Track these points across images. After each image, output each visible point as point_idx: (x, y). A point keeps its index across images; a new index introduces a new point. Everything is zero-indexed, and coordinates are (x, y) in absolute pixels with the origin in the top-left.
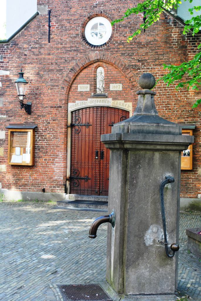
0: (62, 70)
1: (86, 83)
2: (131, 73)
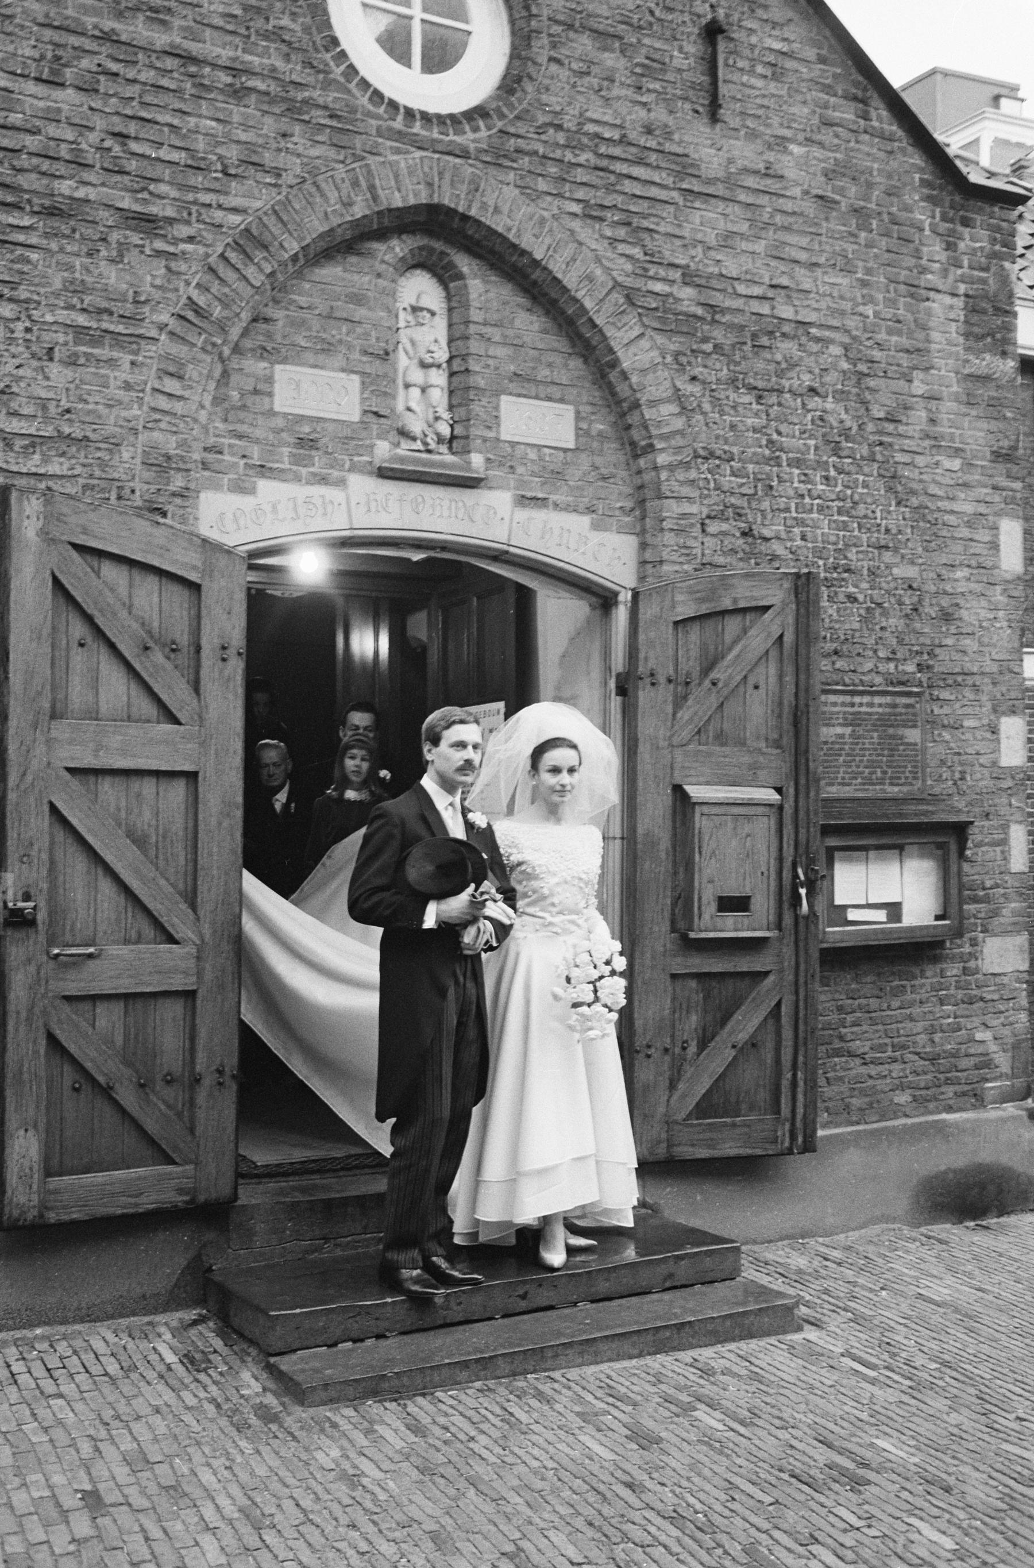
0: (171, 221)
1: (339, 360)
2: (645, 343)
